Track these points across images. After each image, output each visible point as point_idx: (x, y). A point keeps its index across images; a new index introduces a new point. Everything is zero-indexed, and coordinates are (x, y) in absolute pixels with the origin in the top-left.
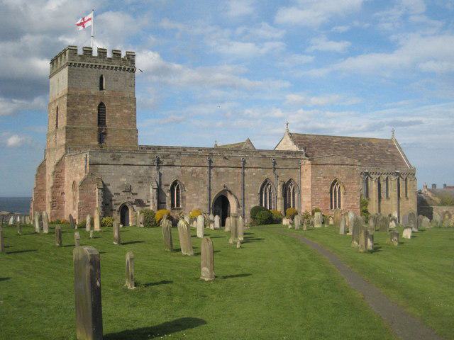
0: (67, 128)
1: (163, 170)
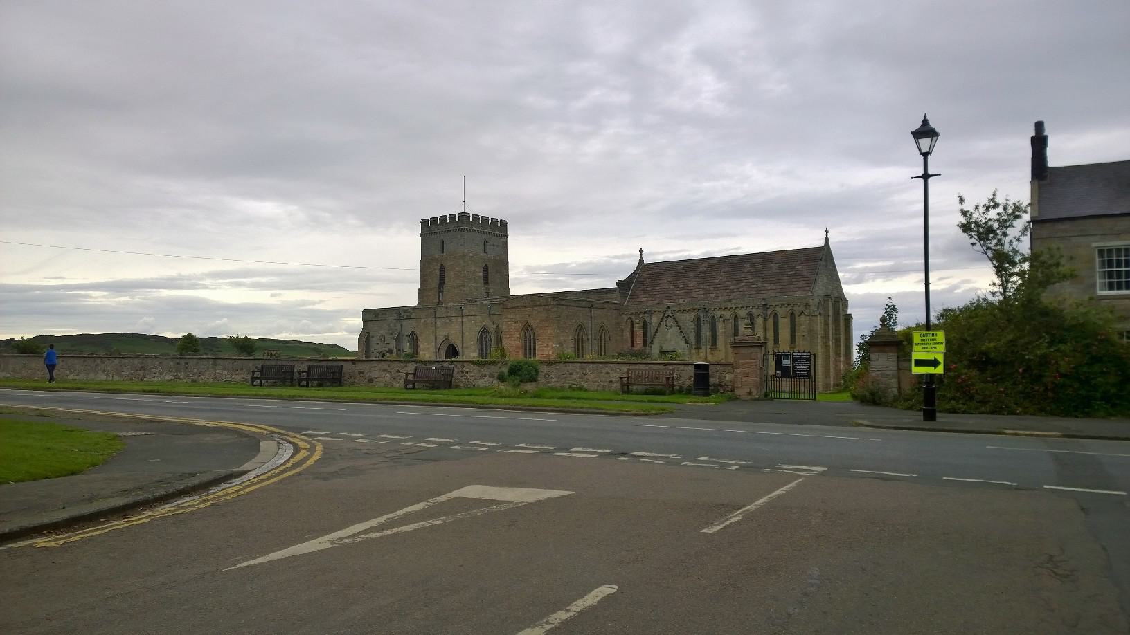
1: (405, 323)
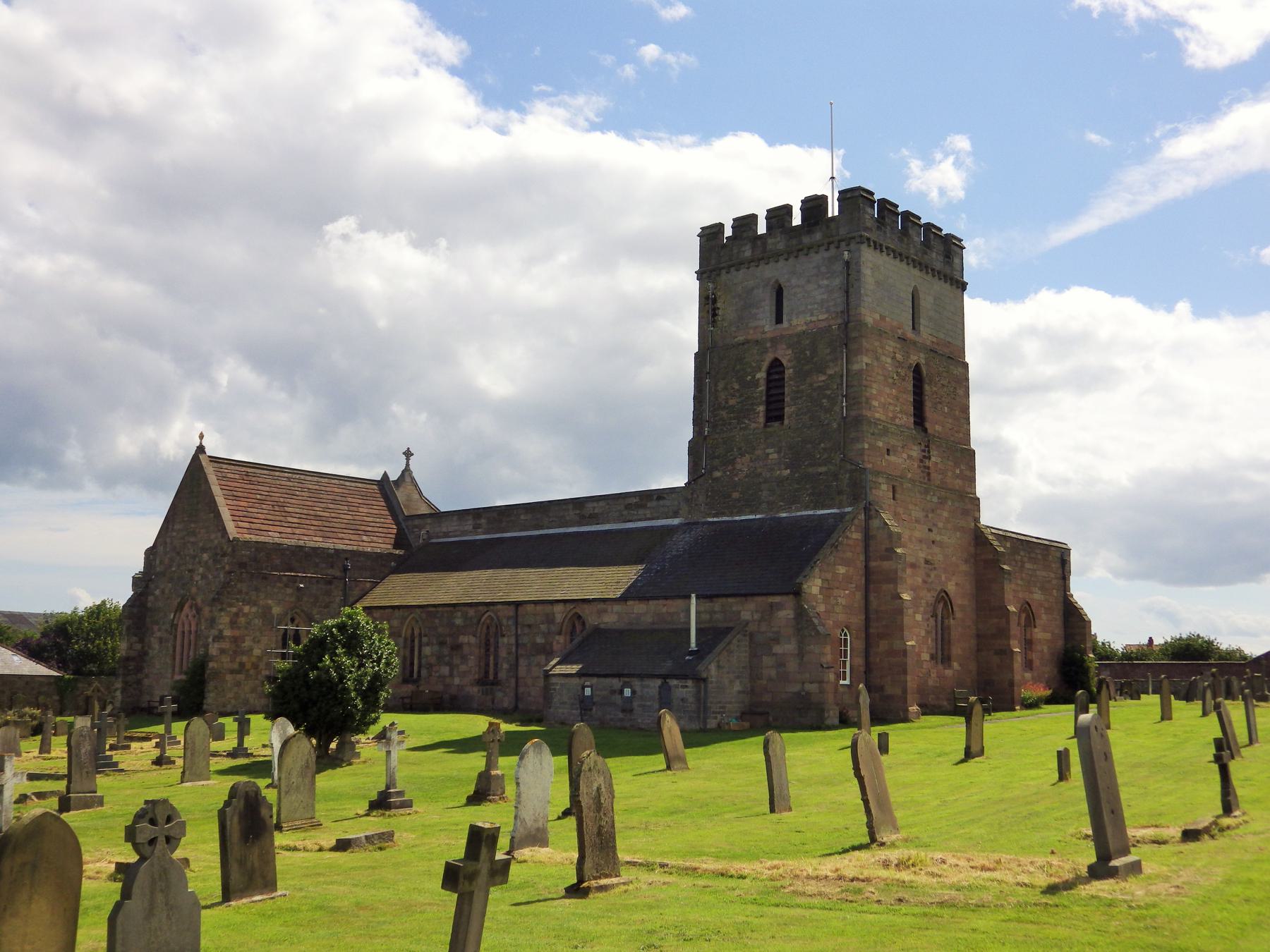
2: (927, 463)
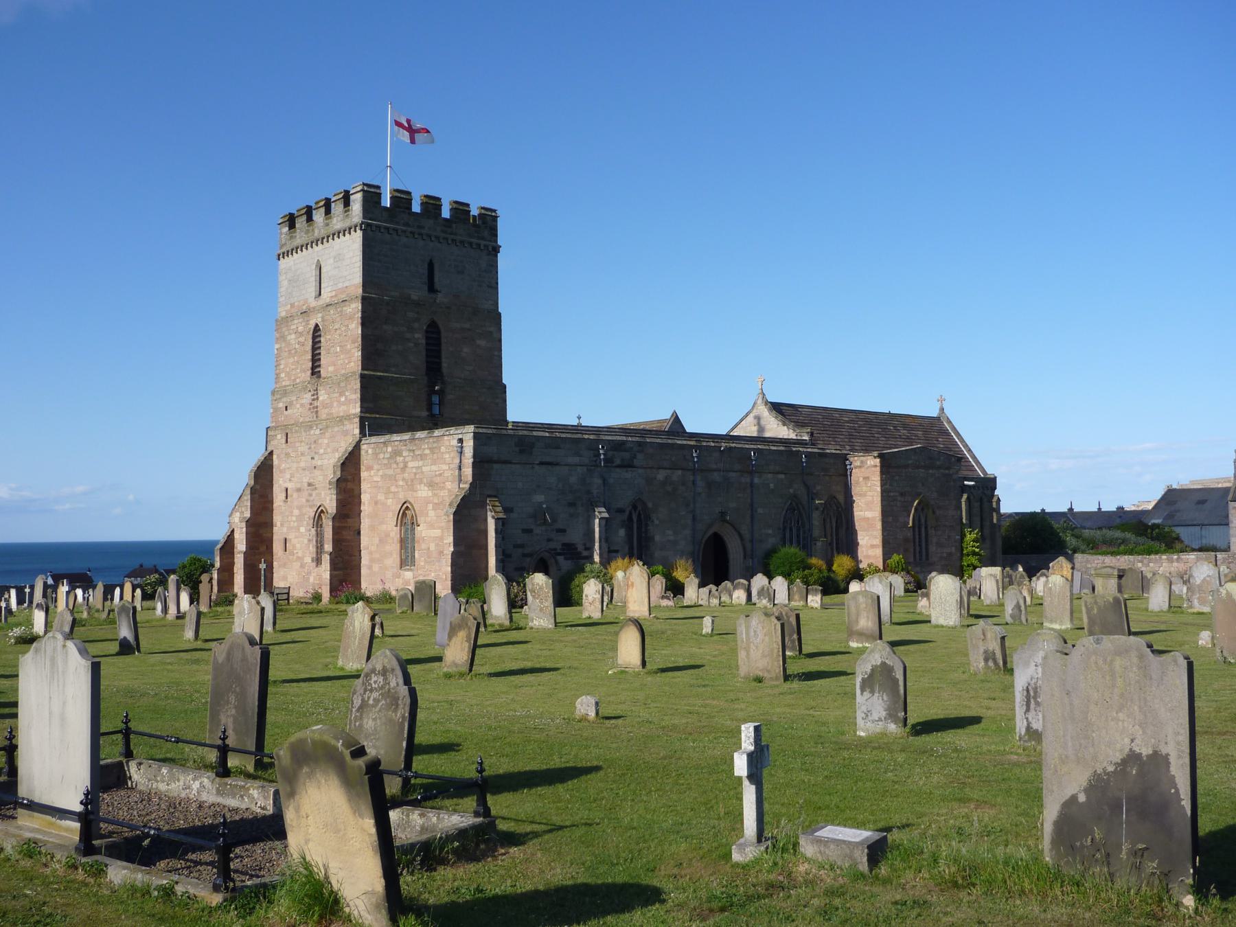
0: (362, 377)
2: (315, 403)
